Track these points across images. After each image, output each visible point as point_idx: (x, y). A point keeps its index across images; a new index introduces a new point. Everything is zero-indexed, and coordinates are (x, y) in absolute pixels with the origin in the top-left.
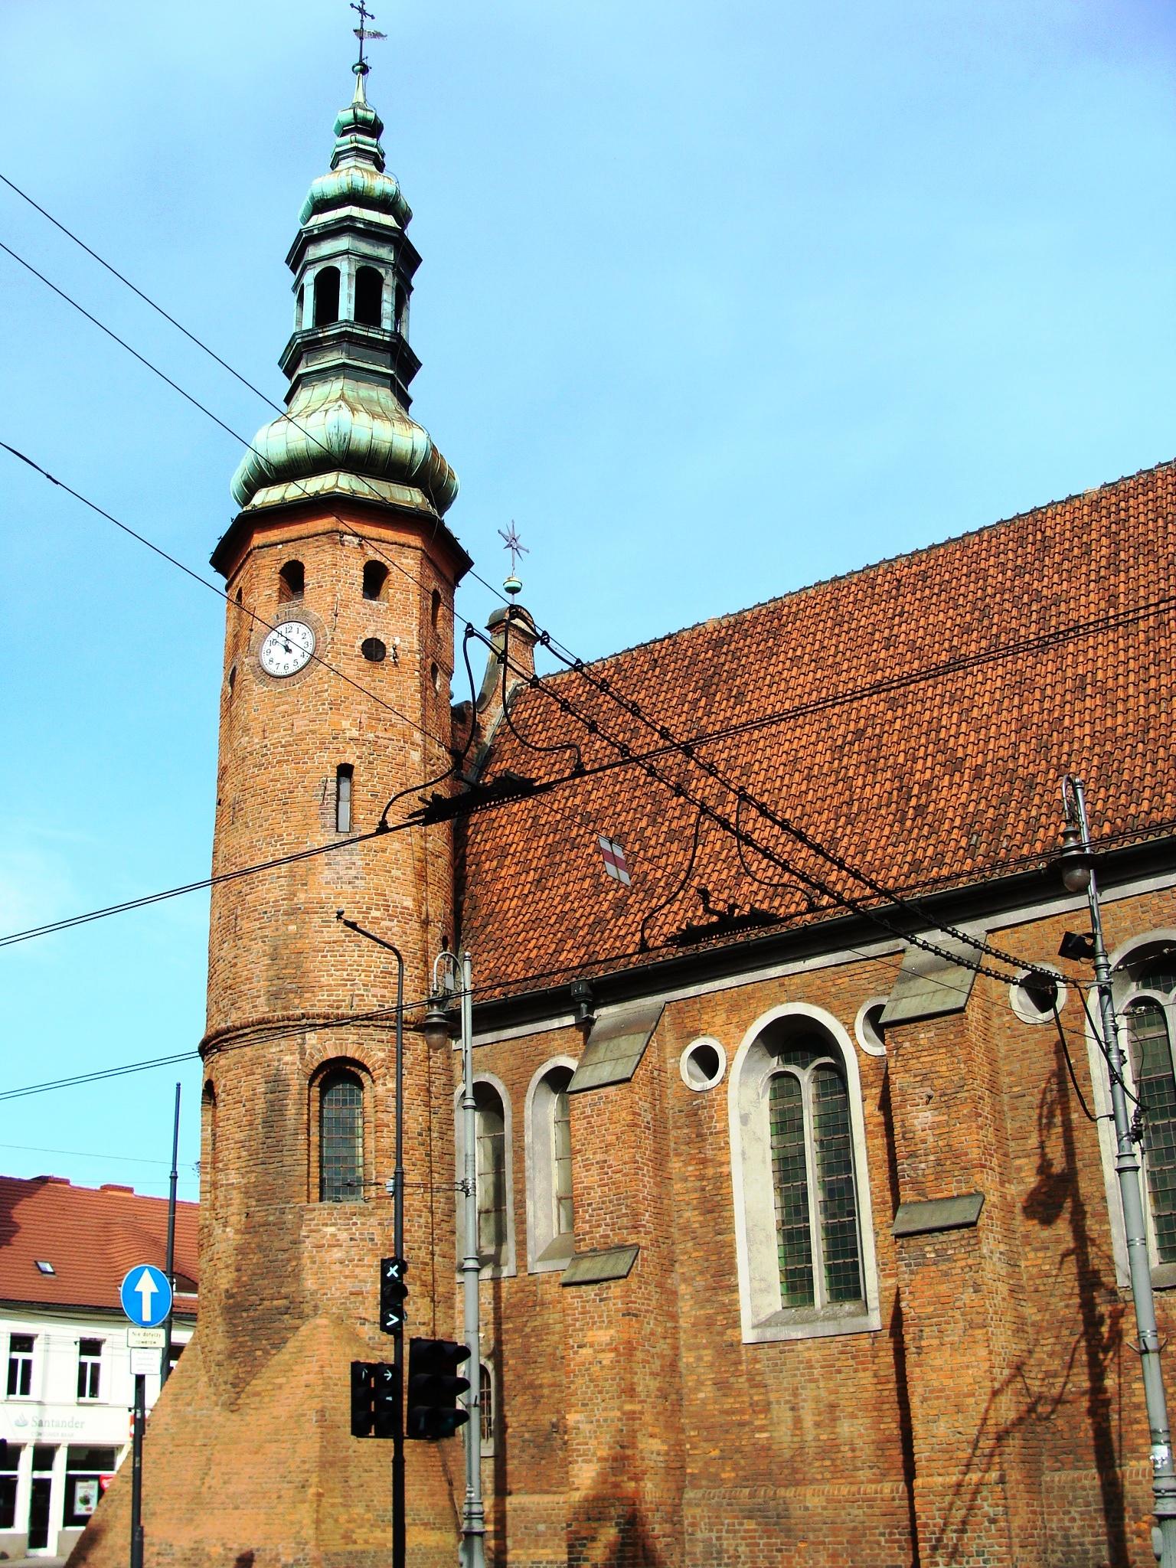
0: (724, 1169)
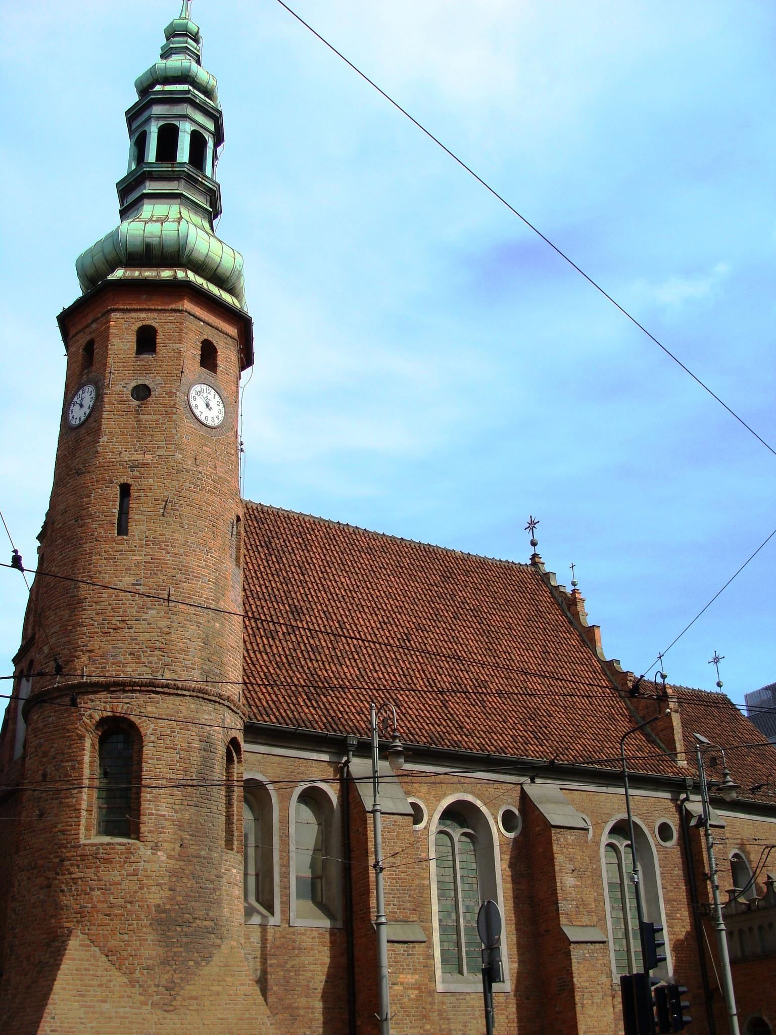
0: (426, 882)
